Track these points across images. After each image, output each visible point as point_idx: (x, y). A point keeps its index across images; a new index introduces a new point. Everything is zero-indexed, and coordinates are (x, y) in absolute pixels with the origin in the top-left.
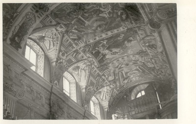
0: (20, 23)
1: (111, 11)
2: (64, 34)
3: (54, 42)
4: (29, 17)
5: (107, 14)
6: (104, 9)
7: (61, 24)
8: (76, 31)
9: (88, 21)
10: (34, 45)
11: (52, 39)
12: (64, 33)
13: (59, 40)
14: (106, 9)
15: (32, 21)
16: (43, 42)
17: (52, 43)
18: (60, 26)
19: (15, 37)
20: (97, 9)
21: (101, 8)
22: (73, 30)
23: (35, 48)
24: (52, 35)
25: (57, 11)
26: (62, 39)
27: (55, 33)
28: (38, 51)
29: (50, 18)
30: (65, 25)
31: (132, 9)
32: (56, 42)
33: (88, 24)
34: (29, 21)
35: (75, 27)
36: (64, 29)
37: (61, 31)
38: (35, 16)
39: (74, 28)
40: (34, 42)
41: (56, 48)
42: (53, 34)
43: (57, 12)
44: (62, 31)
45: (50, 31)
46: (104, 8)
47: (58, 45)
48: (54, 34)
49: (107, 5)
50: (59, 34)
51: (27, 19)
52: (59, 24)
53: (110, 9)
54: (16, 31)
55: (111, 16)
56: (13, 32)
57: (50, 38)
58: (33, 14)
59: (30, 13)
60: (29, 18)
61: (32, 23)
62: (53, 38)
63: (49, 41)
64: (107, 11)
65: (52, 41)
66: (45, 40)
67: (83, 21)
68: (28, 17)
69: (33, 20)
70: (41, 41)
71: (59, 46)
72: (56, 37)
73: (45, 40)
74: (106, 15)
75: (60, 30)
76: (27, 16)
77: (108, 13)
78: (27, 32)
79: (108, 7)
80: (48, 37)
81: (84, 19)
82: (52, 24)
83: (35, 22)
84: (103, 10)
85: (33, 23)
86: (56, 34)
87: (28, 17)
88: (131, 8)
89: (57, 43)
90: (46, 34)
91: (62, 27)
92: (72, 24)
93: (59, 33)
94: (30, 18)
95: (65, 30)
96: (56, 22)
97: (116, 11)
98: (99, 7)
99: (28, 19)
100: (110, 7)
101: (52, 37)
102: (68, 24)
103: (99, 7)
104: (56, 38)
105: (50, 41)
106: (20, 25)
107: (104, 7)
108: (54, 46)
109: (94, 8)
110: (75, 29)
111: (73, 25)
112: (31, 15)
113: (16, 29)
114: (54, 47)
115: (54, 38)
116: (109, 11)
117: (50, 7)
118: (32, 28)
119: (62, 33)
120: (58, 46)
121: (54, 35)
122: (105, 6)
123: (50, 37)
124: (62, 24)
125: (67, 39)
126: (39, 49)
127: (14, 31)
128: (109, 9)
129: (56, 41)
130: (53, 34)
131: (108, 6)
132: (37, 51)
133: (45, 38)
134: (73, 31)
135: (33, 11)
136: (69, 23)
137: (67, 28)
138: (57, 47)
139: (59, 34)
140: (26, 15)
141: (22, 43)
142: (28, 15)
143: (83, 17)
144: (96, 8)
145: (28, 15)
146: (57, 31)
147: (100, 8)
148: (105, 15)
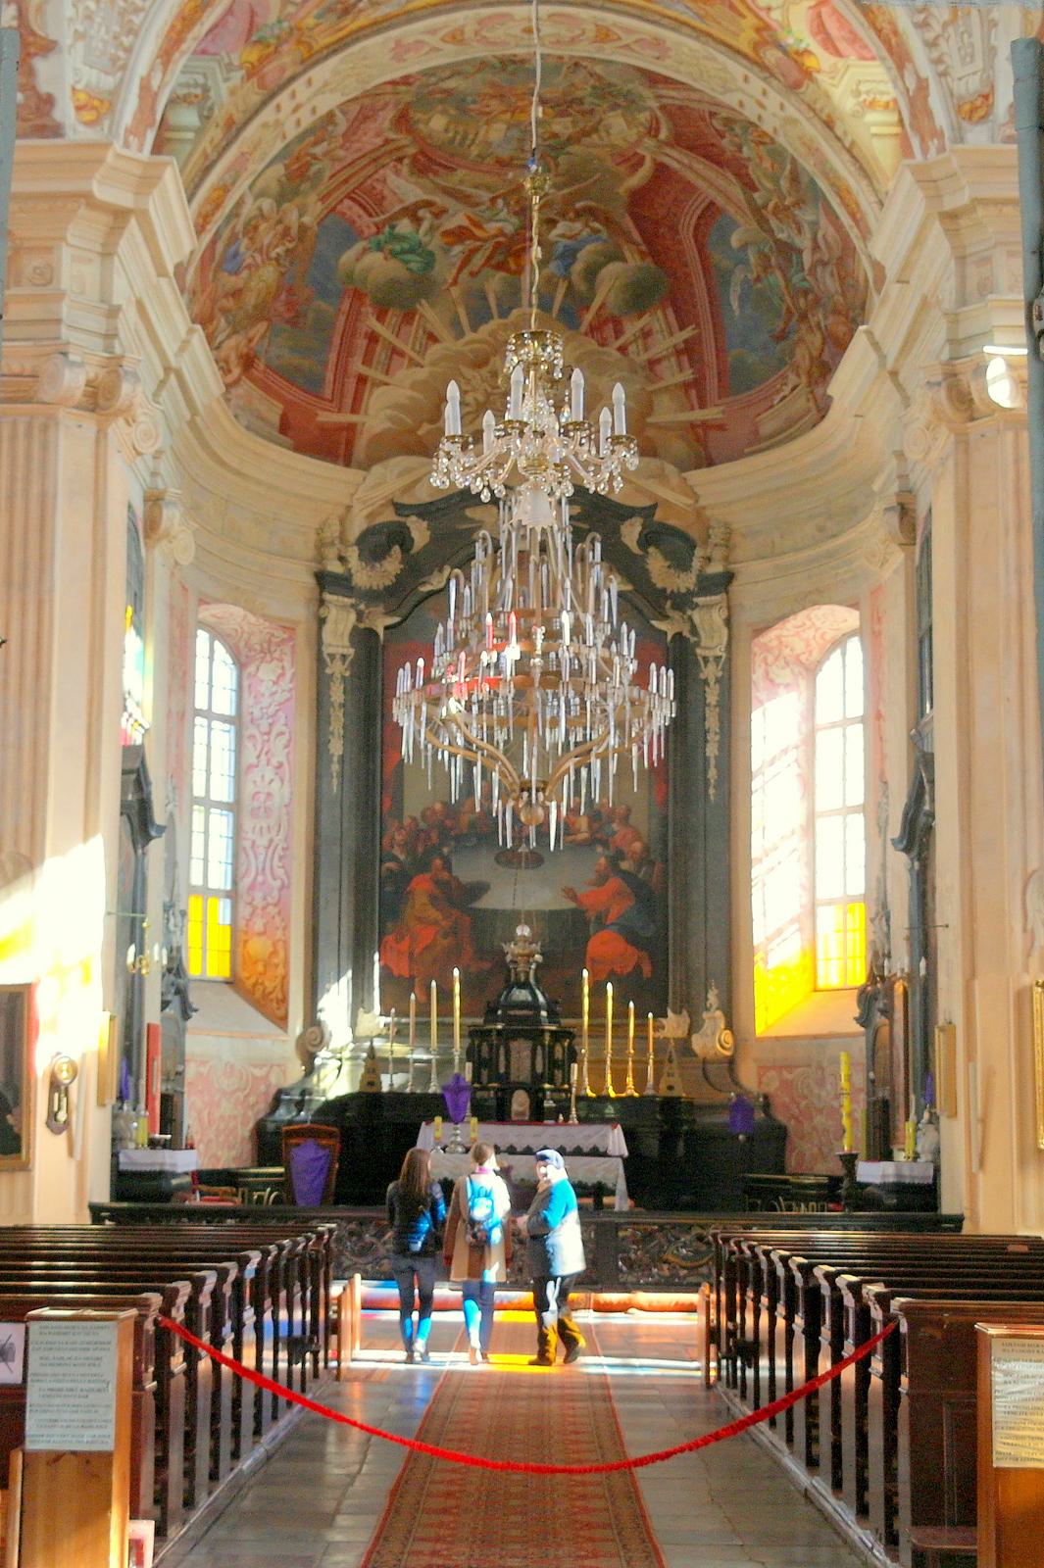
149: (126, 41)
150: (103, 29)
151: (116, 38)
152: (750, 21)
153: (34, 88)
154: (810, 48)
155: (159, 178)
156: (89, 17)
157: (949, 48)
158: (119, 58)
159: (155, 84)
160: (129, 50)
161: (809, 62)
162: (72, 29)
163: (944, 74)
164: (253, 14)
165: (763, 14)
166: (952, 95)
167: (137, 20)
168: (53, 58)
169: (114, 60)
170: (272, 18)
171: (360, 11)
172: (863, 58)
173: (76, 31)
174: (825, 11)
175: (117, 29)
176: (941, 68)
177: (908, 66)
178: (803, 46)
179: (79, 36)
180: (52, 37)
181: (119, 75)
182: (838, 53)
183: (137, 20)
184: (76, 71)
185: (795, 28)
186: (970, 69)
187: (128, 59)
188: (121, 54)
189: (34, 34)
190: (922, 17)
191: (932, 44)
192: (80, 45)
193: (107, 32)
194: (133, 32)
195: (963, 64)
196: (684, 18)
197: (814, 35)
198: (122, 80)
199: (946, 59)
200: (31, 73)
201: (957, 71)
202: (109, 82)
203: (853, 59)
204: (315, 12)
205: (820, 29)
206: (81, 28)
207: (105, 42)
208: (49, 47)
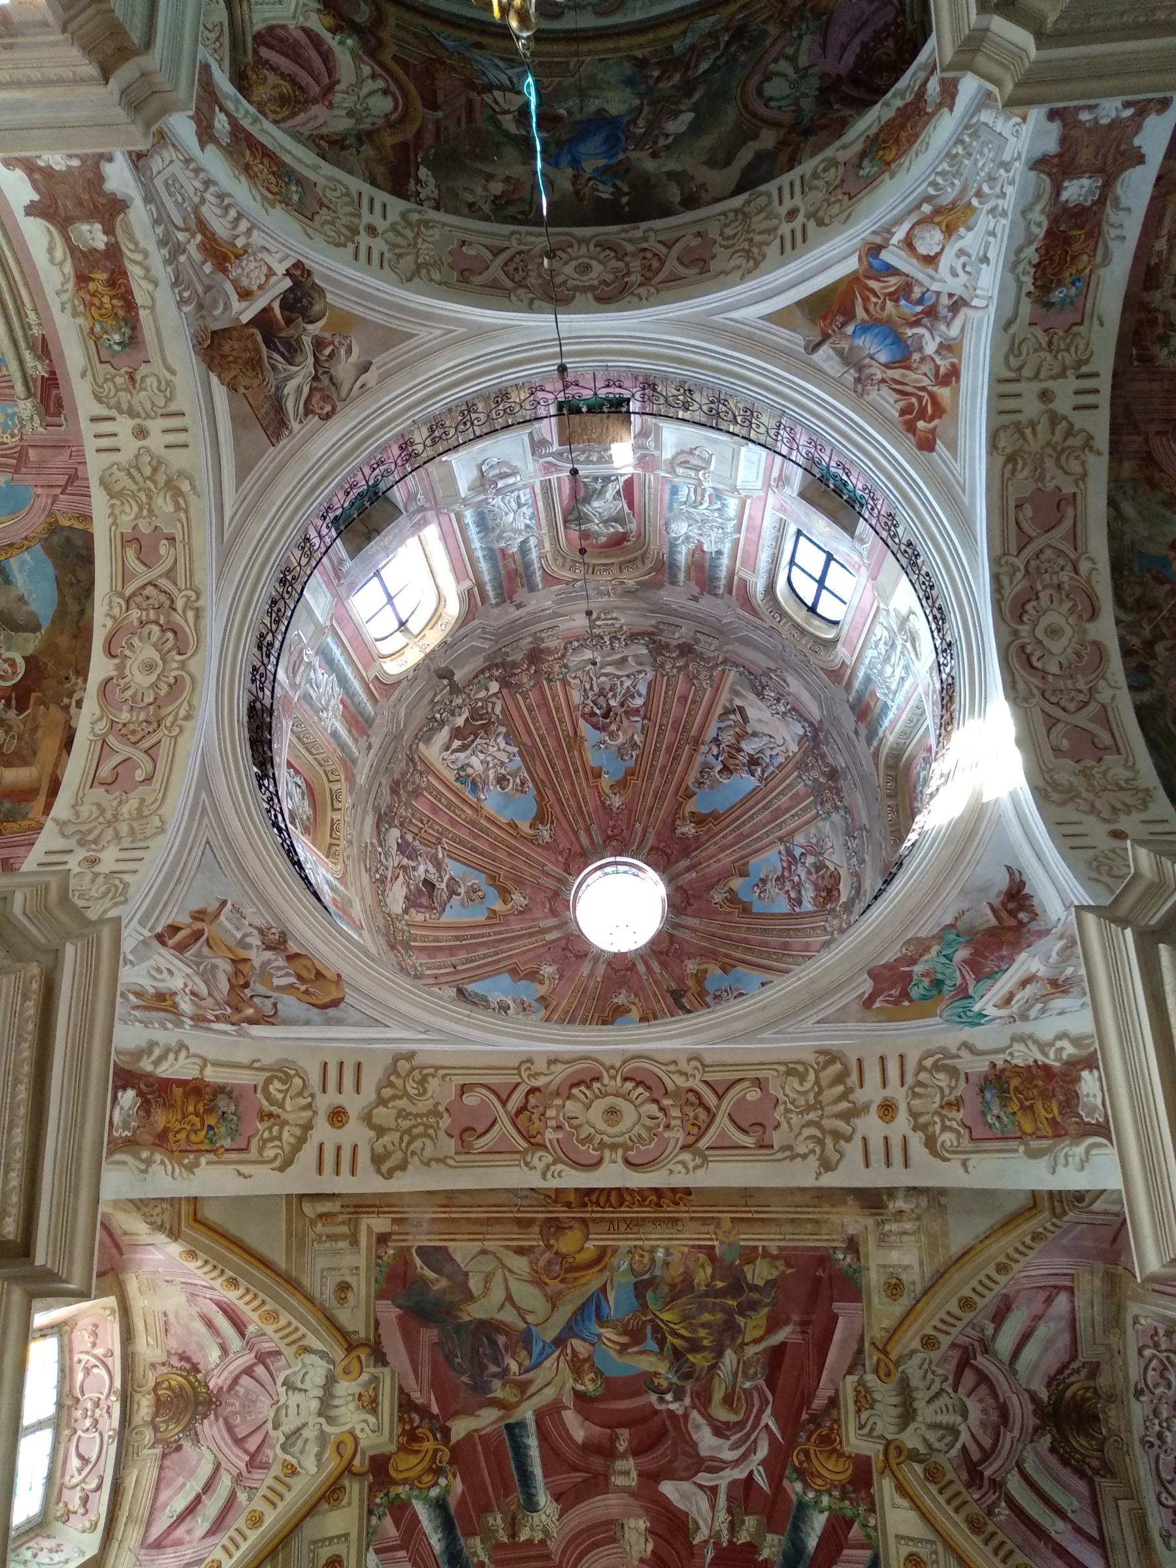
0: (215, 1064)
1: (761, 1480)
2: (348, 1470)
3: (242, 1497)
4: (280, 1096)
5: (722, 1501)
6: (716, 1441)
7: (385, 1363)
8: (436, 1541)
9: (557, 1498)
10: (96, 1422)
11: (240, 1461)
12: (357, 1462)
13: (289, 1496)
14: (731, 1449)
15: (272, 1139)
16: (166, 1443)
17: (212, 1507)
18: (369, 1382)
19: (133, 1087)
20: (671, 1413)
21: (701, 1420)
22: (424, 1499)
23: (81, 1457)
24: (269, 1425)
25: (421, 1251)
26: (311, 1510)
27: (299, 1429)
28: (75, 1502)
29: (361, 1261)
30: (400, 1406)
31: (933, 1489)
32: (259, 1505)
33: (545, 1531)
34: (261, 1120)
35: (447, 1490)
36: (377, 1430)
37: (352, 1433)
38: (307, 1127)
39: (434, 1492)
40: (118, 1384)
41: (219, 1554)
42: (276, 1427)
43: (418, 1262)
44: (356, 1440)
45: (280, 1381)
46: (720, 1430)
47: (253, 1535)
48: (288, 1425)
49: (757, 1403)
50: (319, 1456)
51: (259, 1095)
52: (381, 1358)
53: (763, 1451)
54: (167, 1070)
55: (743, 1538)
56: (152, 1045)
57: (239, 1442)
58: (309, 1106)
59: (305, 1086)
60: (272, 1102)
61: (261, 1151)
62: (255, 1462)
63: (217, 1467)
64: (737, 1463)
65: (238, 1479)
66: (196, 1440)
67: (526, 1478)
68: (275, 1087)
69: (279, 1138)
70: (156, 1429)
71: (245, 1555)
72: (286, 1465)
73: (196, 1440)
74: (713, 1507)
75: (351, 1417)
76: (280, 1079)
77: (733, 1484)
78: (197, 1164)
79: (753, 1429)
80: (230, 1429)
81: (540, 1446)
82: (336, 1312)
83: (277, 1164)
84: (706, 1441)
85: (269, 1153)
86: (300, 1443)
87: (275, 1087)
88: (925, 1471)
89: (256, 1520)
90: (245, 1380)
91: (372, 1405)
92: (446, 1432)
93: (323, 1437)
94: (274, 1109)
95: (380, 1440)
96: (367, 1332)
97: (798, 1486)
98: (687, 1401)
99: (264, 1103)
100: (767, 1426)
101: (252, 1446)
102: (424, 1411)
103: (687, 1401)
104: (276, 1470)
105: (222, 1471)
106: (212, 1075)
107: (722, 1414)
108: (217, 1526)
109: (653, 1398)
110: (440, 1505)
111: (447, 1455)
112: (303, 1101)
113: (171, 1056)
114: (211, 1541)
115: (265, 1466)
116: (744, 1475)
117: (416, 1158)
118: (240, 1174)
119: (348, 1454)
120: (244, 1546)
121: (282, 1439)
122: (736, 1412)
123: (241, 1432)
124: (393, 1373)
125: (339, 1549)
126: (99, 1487)
127: (157, 1052)
128: (753, 1450)
129: (263, 1491)
130: (276, 1427)
131: (761, 1411)
132: (66, 1494)
133: (205, 1416)
134: (415, 1517)
135: (324, 1091)
136: (435, 1410)
137: (402, 1448)
138: (237, 1547)
139: (315, 1450)
140: (280, 1070)
141: (125, 1163)
142: (286, 1079)
143: (543, 1435)
144: (669, 1397)
145: (286, 1079)
146: (320, 1414)
147: (694, 1414)
148: (705, 1505)
149: (960, 149)
150: (980, 164)
151: (970, 155)
152: (387, 56)
153: (1065, 126)
154: (329, 35)
155: (956, 53)
156: (991, 179)
157: (192, 185)
158: (970, 136)
159: (933, 86)
160: (959, 141)
161: (329, 20)
162: (1011, 174)
163: (188, 161)
164: (824, 46)
165: (378, 70)
166: (173, 145)
167: (945, 166)
168: (1038, 154)
169: (975, 135)
170: (807, 39)
171: (726, 29)
172: (283, 27)
173: (1008, 171)
174: (326, 80)
175: (966, 162)
176: (192, 166)
177: (225, 140)
178: (338, 38)
179: (1007, 166)
180: (1033, 174)
181: (974, 121)
182: (306, 31)
183: (945, 166)
184: (1017, 135)
185: (348, 57)
186: (164, 176)
187: (962, 133)
188: (967, 139)
189: (1049, 174)
190: (227, 201)
191: (207, 183)
192: (1007, 157)
193: (976, 161)
194: (951, 157)
195: (176, 180)
196: (448, 30)
197: (330, 50)
198: (972, 117)
199: (191, 175)
200: (1063, 140)
201: (177, 168)
202: (986, 116)
203: (291, 24)
204: (768, 42)
205: (327, 56)
206: (1002, 172)
207: (981, 153)
208: (1039, 164)
